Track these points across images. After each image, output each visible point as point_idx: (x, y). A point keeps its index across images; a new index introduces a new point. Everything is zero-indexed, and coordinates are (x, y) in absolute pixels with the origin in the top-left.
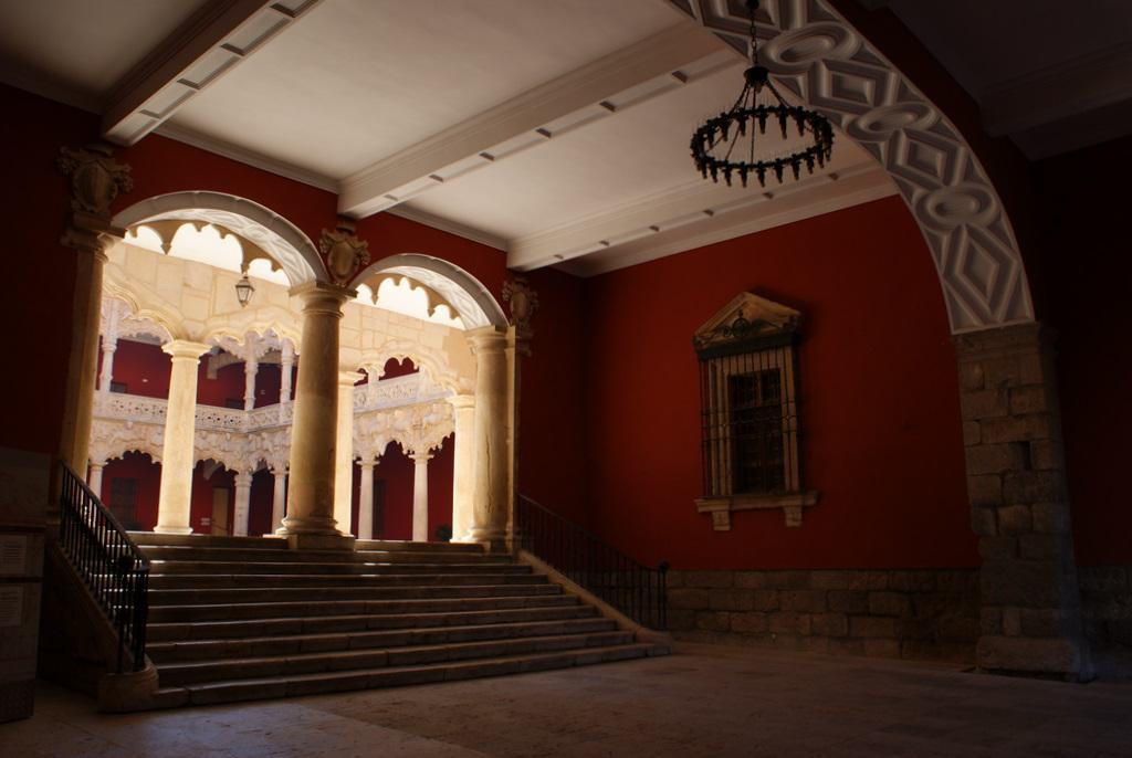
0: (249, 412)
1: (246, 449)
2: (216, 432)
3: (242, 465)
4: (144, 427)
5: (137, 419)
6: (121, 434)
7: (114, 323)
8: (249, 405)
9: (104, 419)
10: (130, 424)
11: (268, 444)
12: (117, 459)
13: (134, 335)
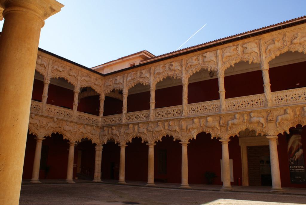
0: (102, 117)
1: (102, 133)
2: (90, 125)
3: (99, 140)
4: (61, 122)
5: (58, 117)
6: (51, 124)
7: (50, 71)
8: (101, 115)
9: (44, 116)
10: (56, 120)
11: (115, 131)
12: (48, 136)
13: (58, 77)
